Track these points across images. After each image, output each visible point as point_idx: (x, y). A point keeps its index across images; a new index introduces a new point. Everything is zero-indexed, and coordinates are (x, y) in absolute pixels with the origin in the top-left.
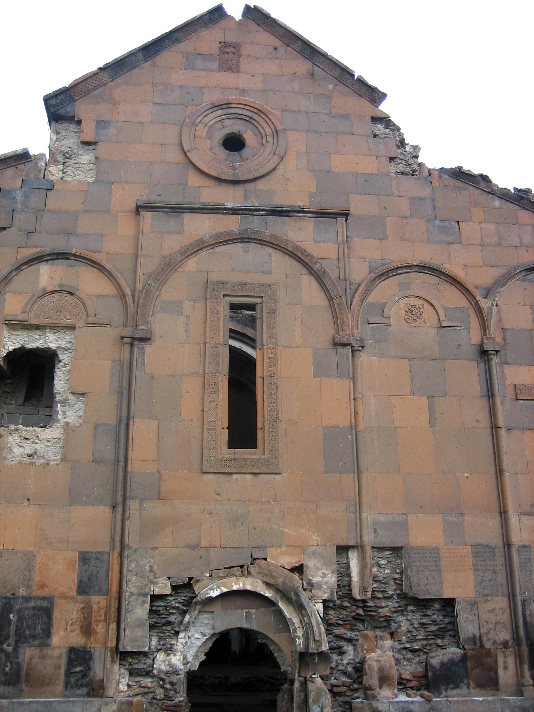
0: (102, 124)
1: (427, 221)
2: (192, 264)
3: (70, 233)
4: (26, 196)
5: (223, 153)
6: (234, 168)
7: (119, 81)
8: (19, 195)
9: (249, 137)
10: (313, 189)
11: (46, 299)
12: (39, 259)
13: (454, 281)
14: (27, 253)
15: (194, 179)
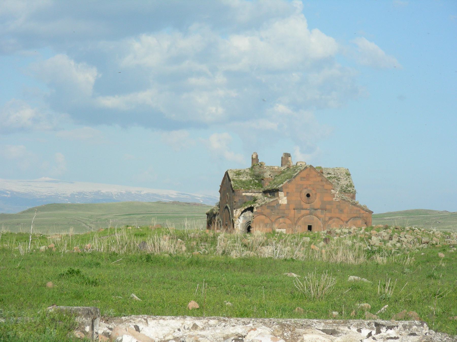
0: (288, 193)
1: (339, 209)
2: (303, 219)
3: (284, 213)
4: (277, 207)
5: (306, 197)
6: (309, 201)
7: (290, 184)
8: (276, 207)
9: (311, 194)
10: (321, 204)
11: (282, 224)
12: (280, 218)
13: (342, 220)
14: (278, 217)
15: (303, 203)
